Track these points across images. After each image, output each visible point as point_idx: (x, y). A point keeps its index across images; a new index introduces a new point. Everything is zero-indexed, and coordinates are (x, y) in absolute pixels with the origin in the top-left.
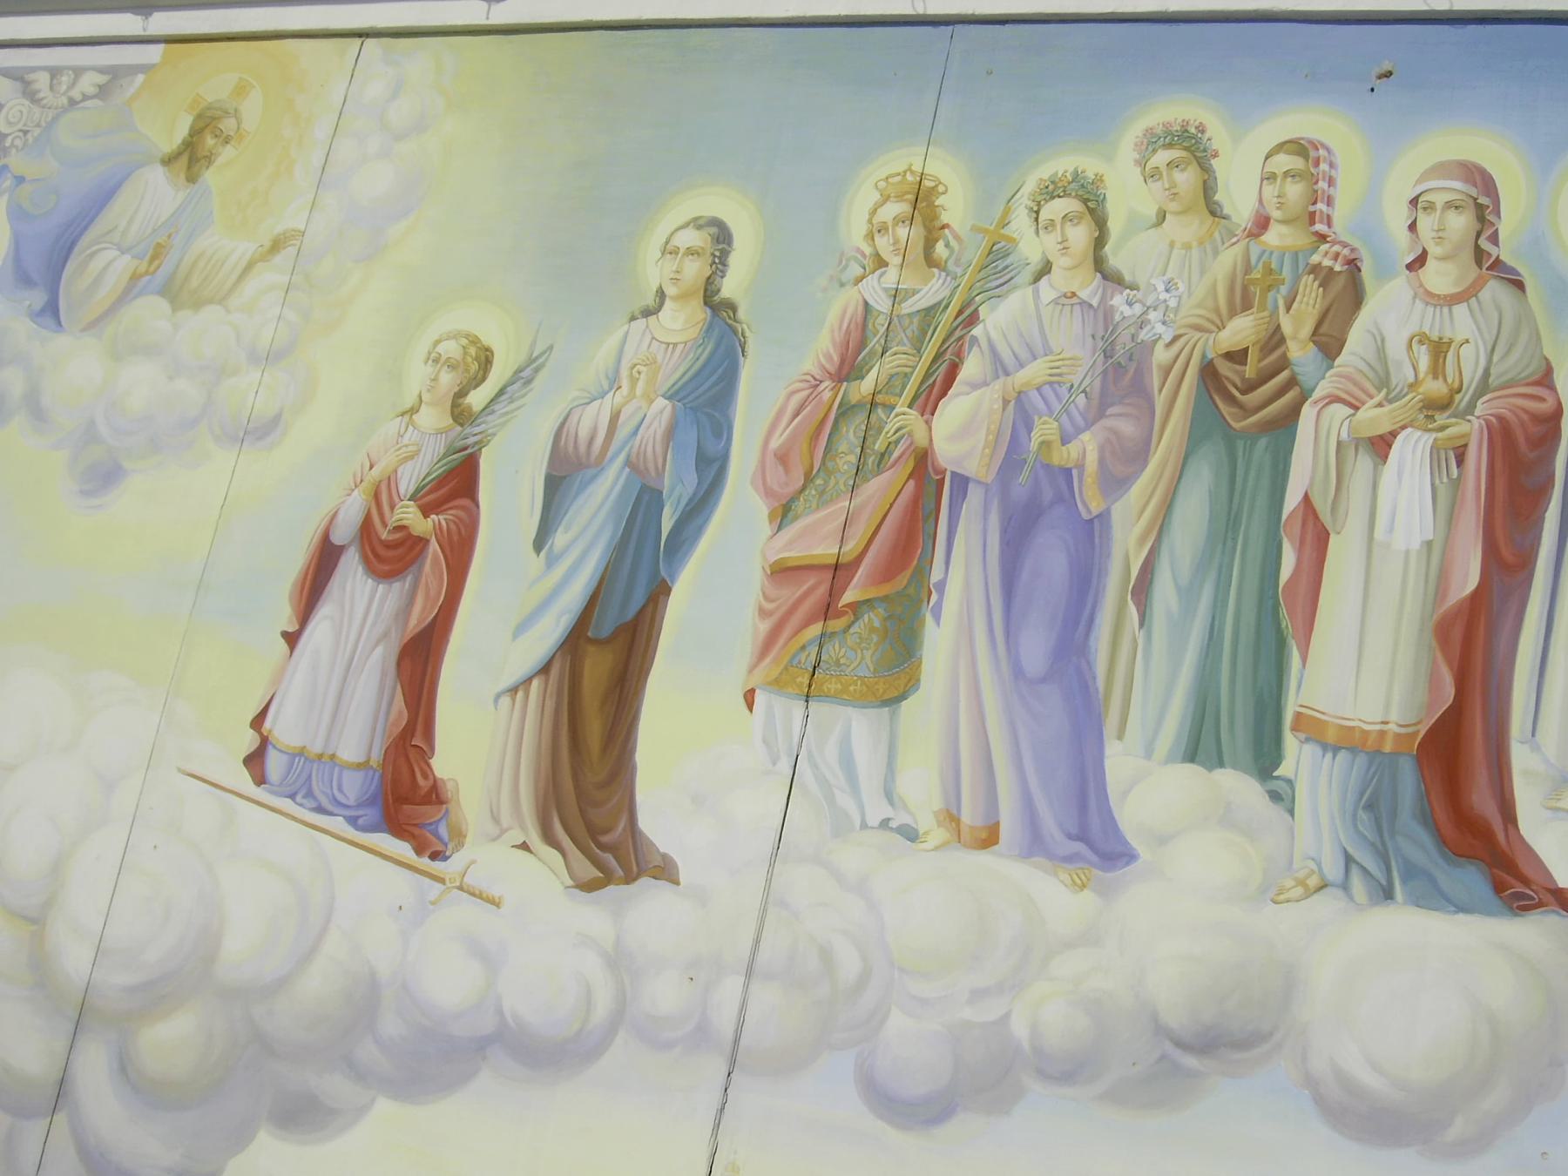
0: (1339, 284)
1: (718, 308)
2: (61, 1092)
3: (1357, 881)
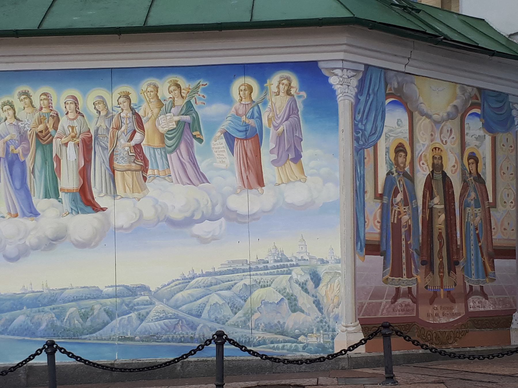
0: (55, 118)
3: (74, 212)
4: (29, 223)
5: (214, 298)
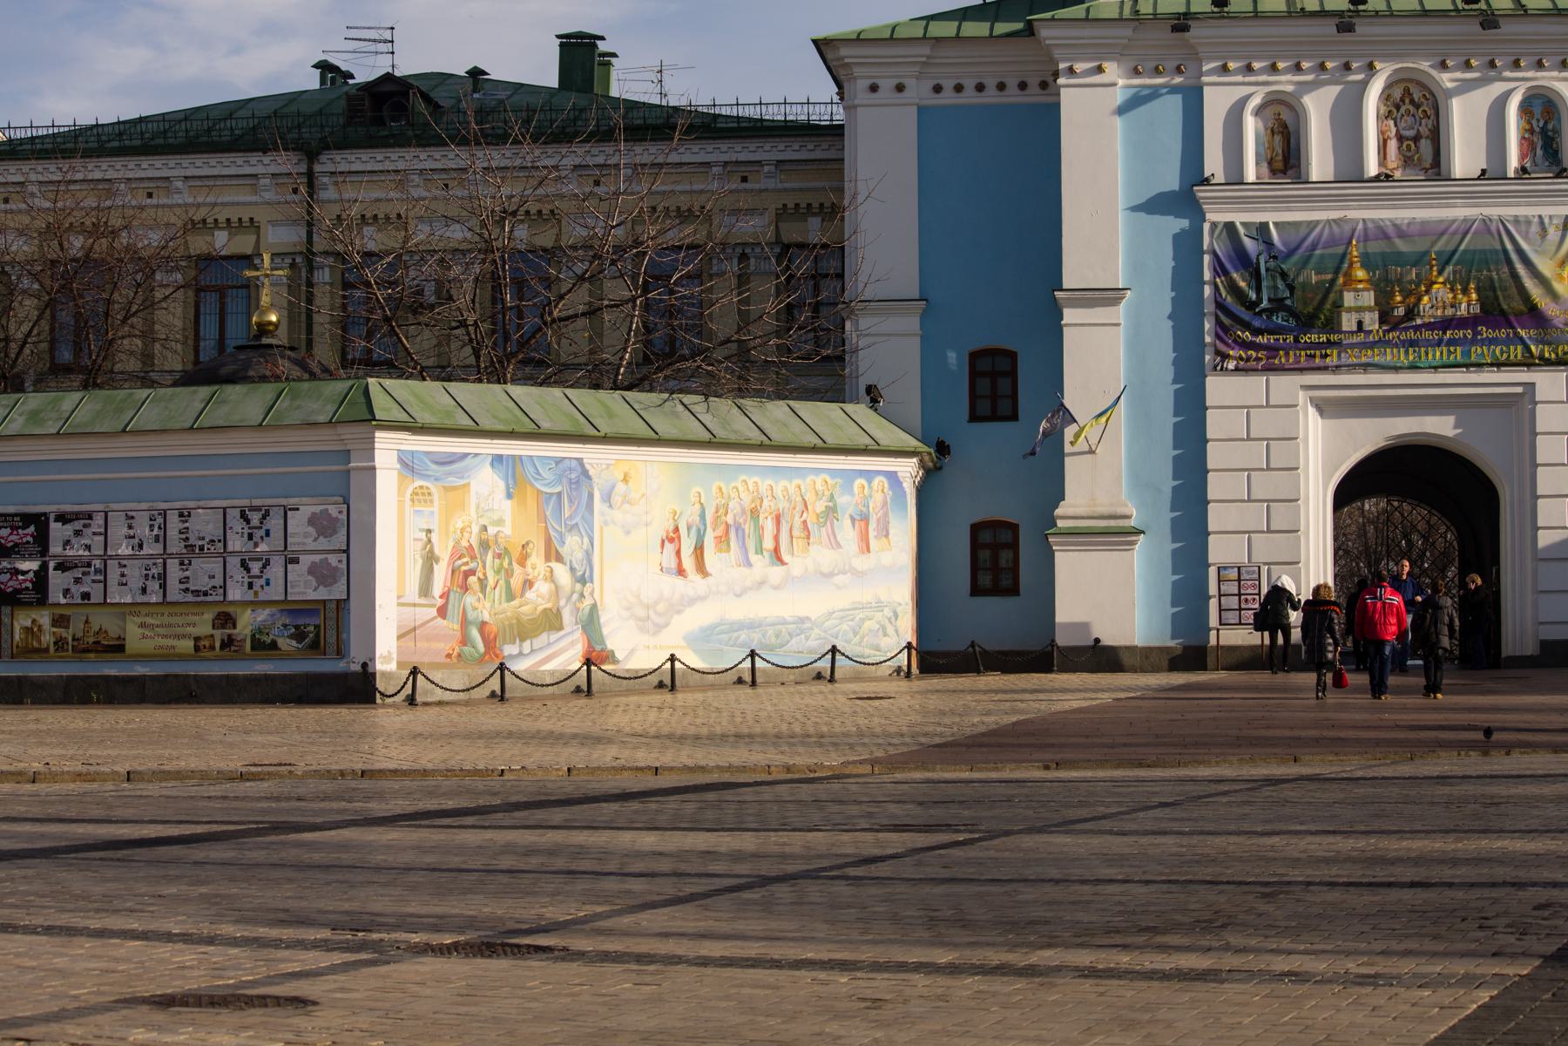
1: (702, 504)
2: (648, 617)
4: (745, 570)
5: (845, 627)
